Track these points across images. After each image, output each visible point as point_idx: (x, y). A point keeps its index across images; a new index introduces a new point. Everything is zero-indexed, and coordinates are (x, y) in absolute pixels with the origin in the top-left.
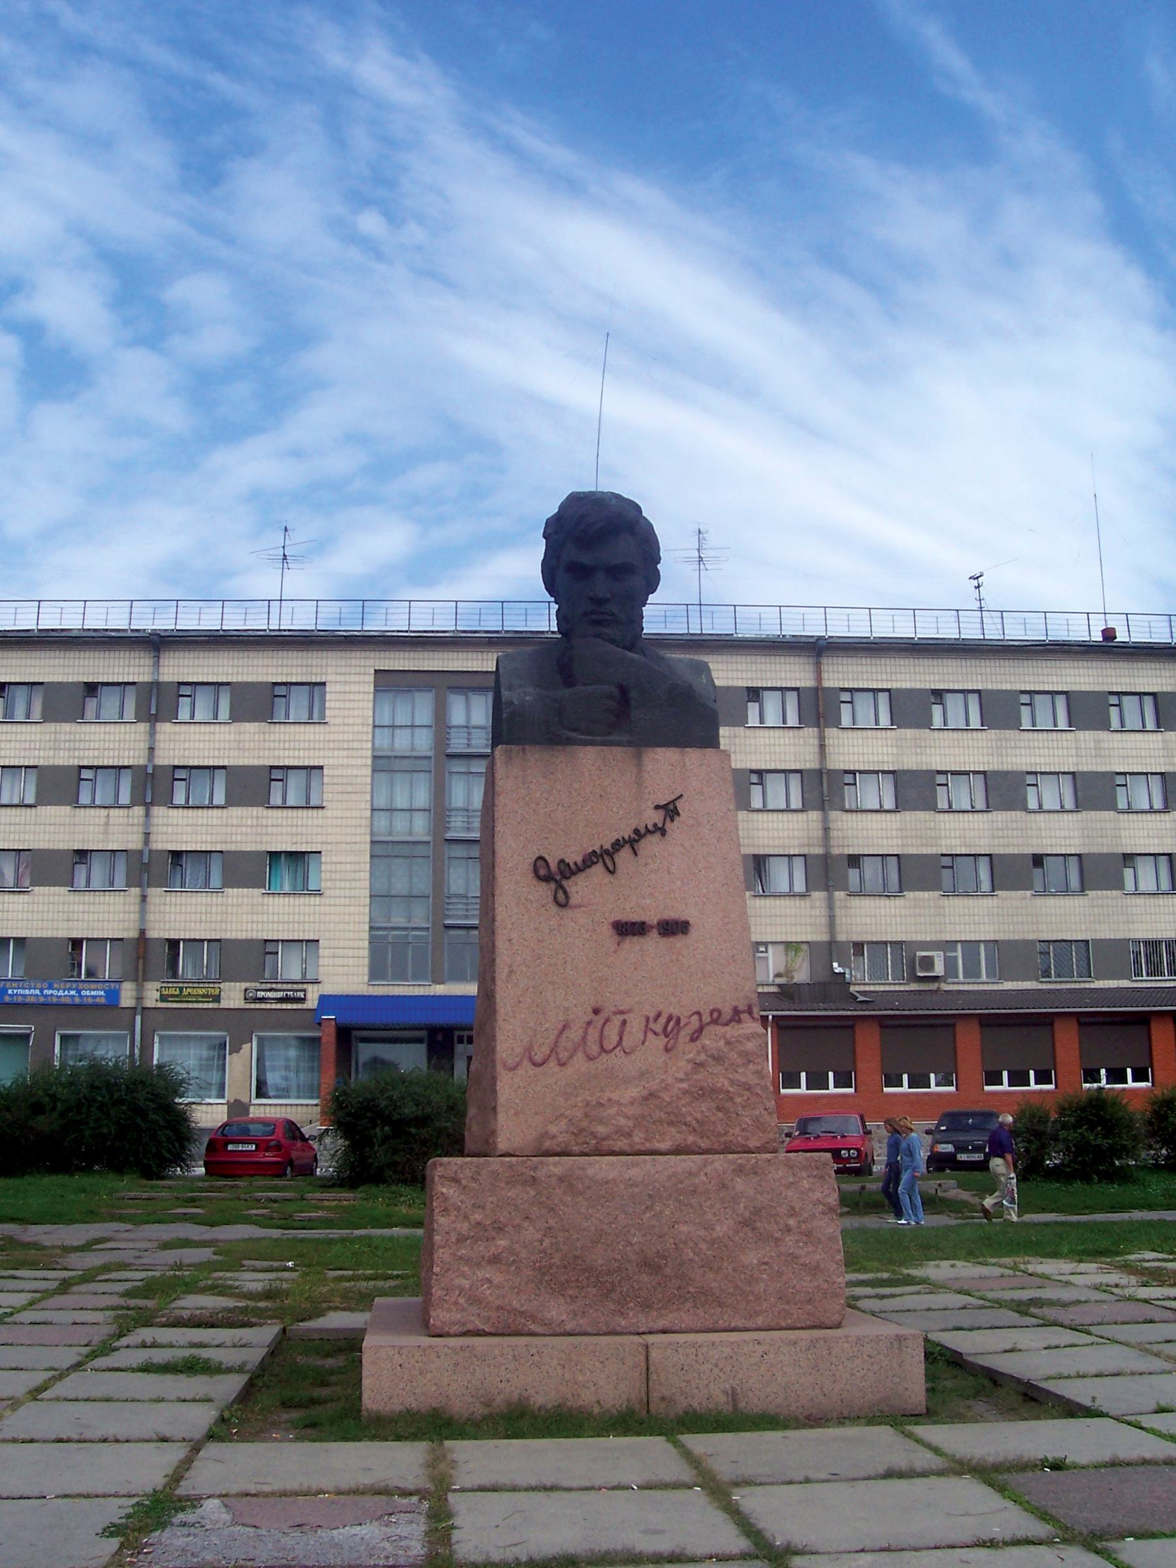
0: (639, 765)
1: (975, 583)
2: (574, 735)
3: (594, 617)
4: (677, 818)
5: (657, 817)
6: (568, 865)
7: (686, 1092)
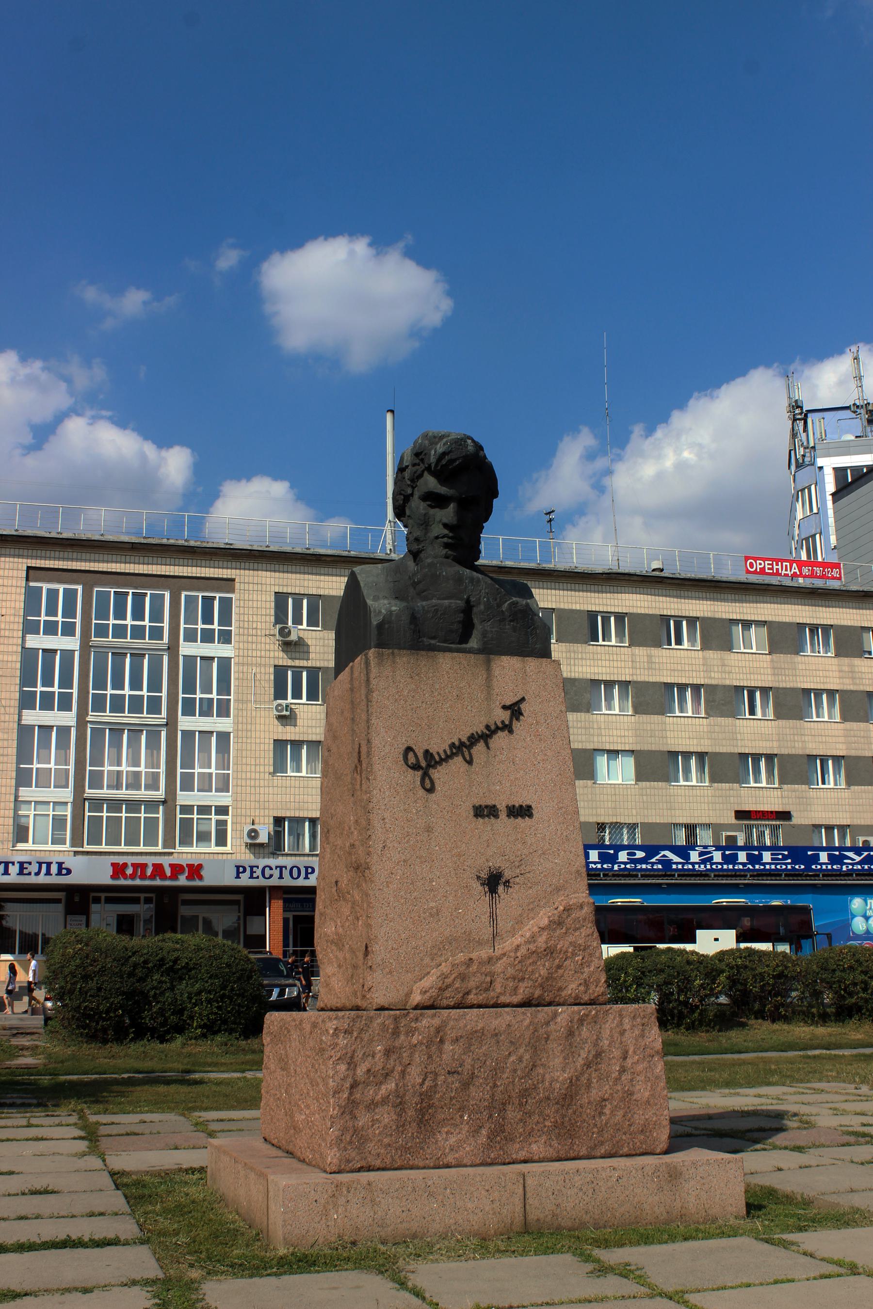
0: (488, 669)
1: (547, 518)
2: (433, 642)
3: (445, 540)
5: (505, 716)
6: (432, 754)
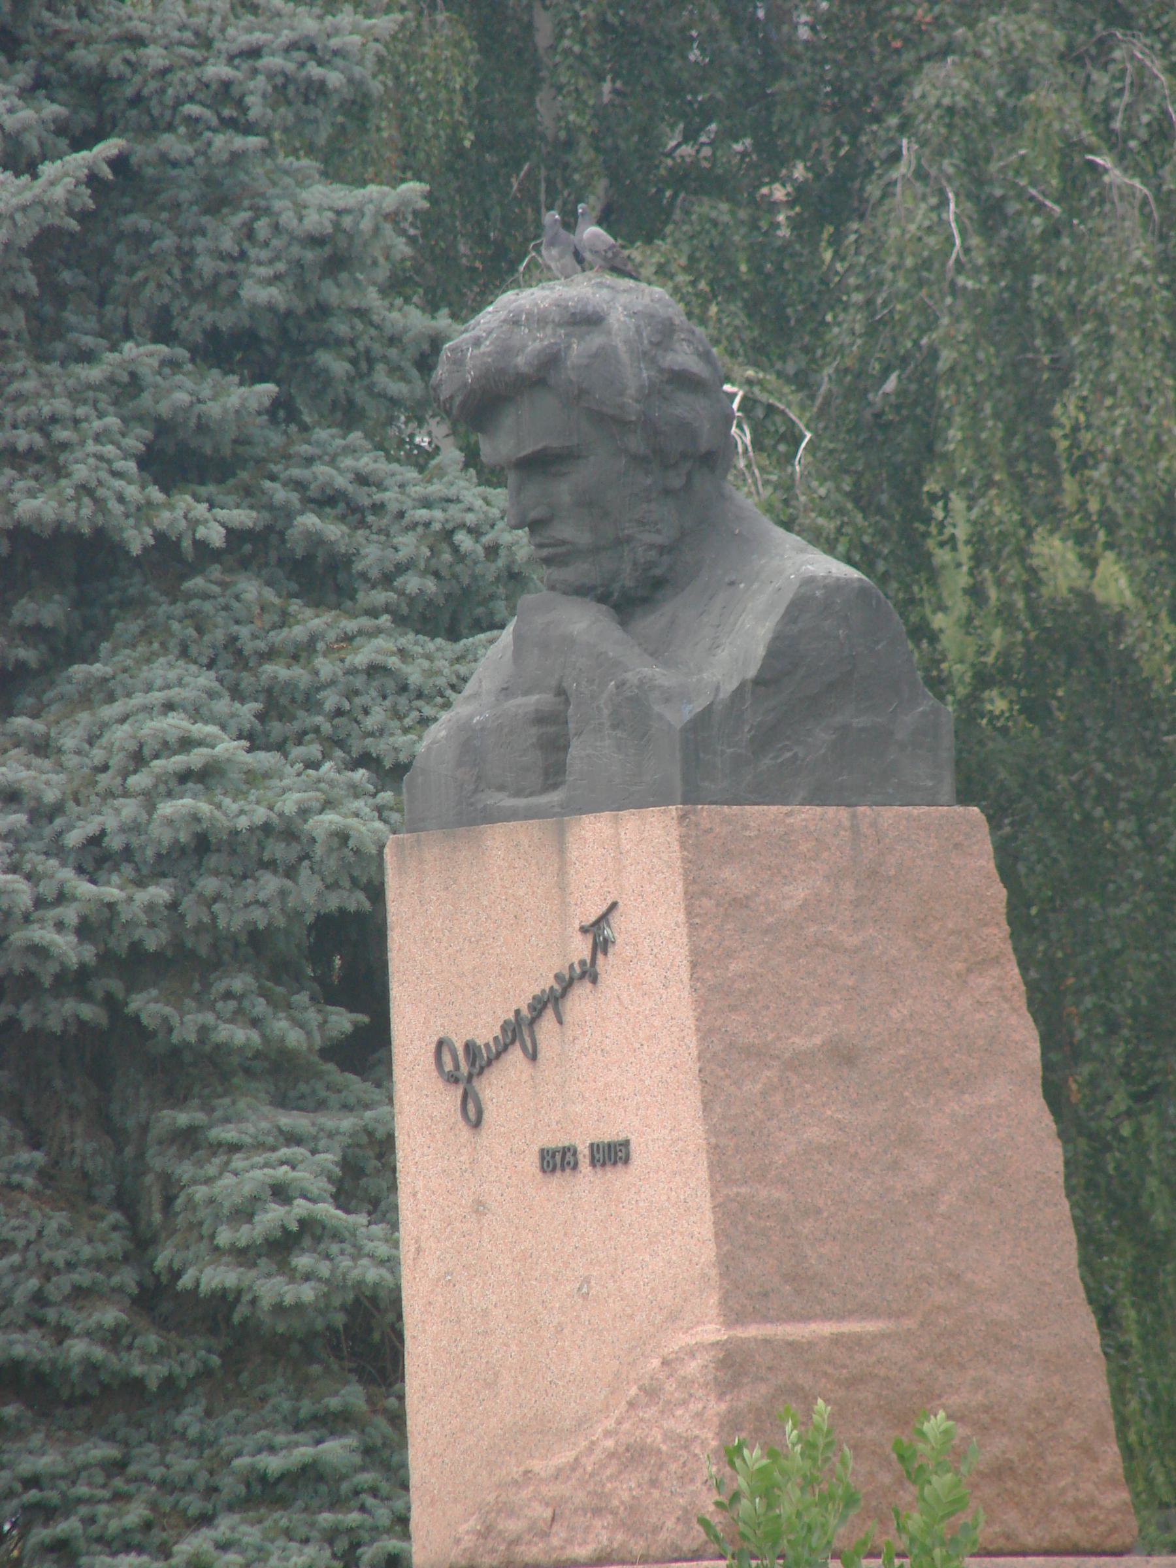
0: (562, 851)
4: (611, 950)
7: (612, 1455)
